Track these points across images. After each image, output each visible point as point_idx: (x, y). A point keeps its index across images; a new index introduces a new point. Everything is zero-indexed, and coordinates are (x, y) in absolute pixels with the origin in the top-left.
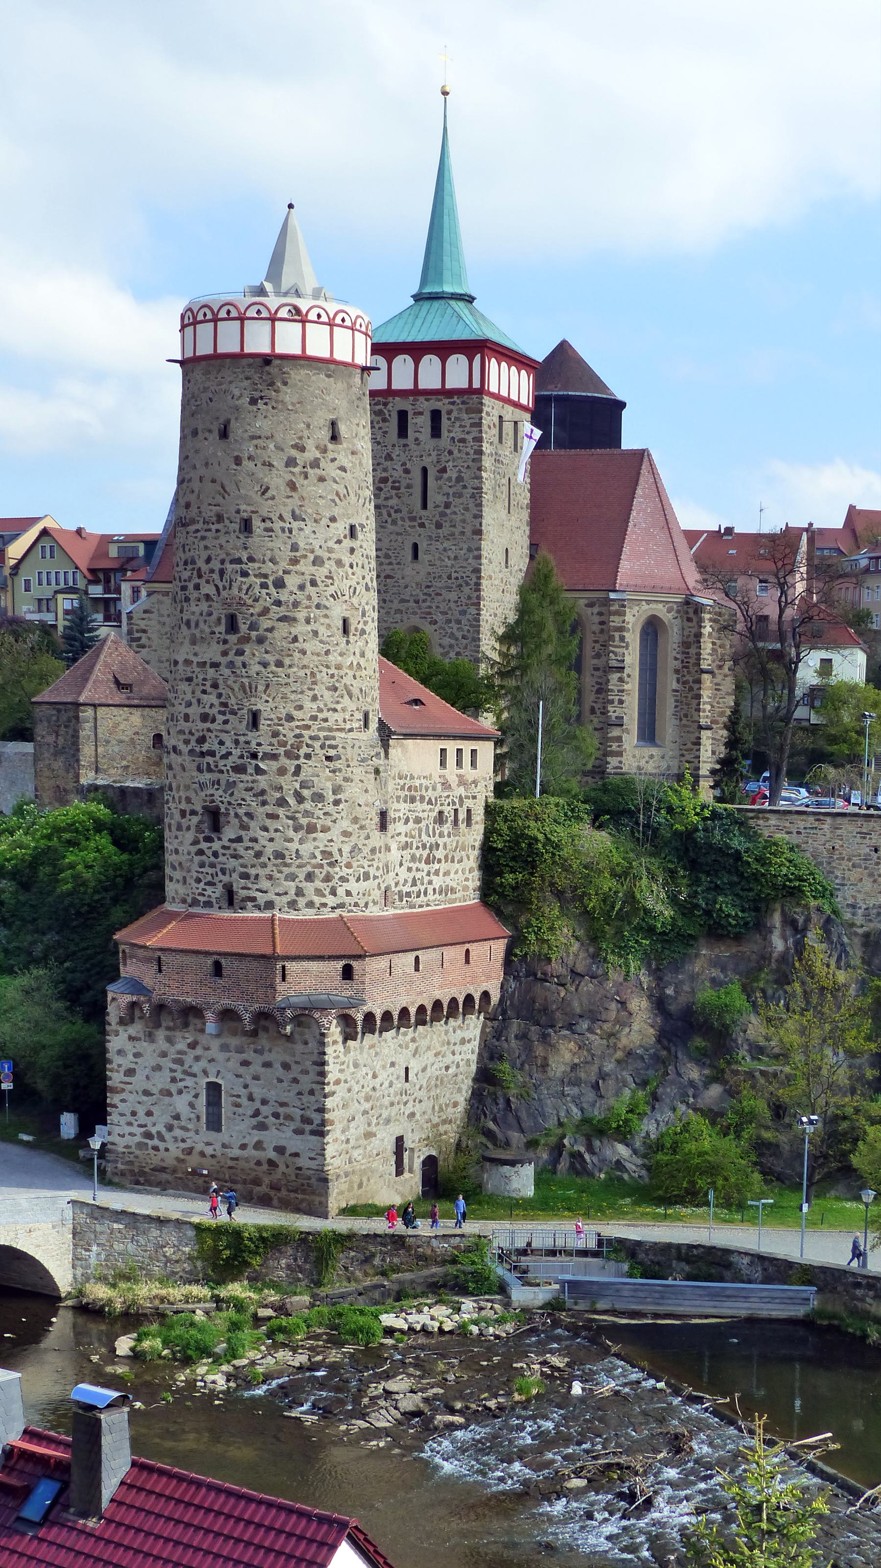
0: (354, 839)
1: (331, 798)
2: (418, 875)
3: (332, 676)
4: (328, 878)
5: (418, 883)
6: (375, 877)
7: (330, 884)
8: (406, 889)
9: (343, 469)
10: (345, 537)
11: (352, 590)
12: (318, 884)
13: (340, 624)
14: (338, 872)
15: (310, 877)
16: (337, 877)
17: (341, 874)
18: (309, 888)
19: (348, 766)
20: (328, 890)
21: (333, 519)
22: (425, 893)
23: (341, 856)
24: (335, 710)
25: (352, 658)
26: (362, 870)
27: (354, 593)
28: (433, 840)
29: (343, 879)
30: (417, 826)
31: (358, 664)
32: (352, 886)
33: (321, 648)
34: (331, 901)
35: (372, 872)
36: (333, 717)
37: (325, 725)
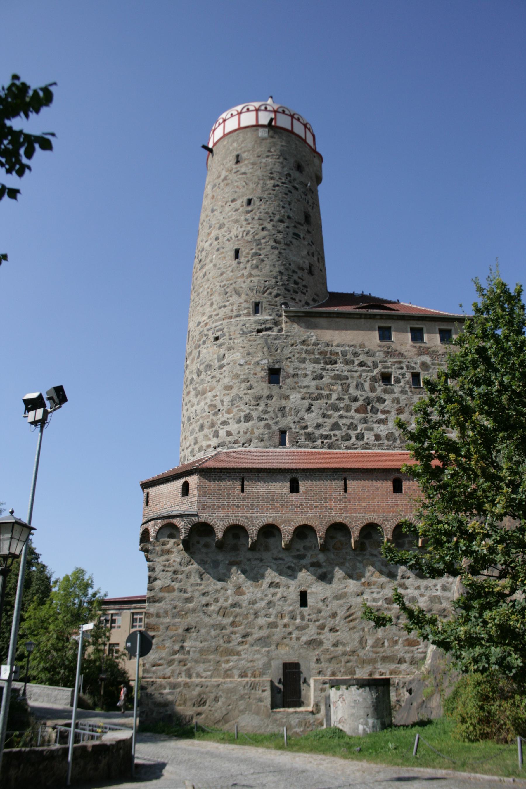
0: (234, 391)
1: (216, 364)
2: (341, 422)
3: (224, 286)
4: (213, 425)
5: (344, 429)
6: (261, 419)
7: (214, 429)
8: (323, 431)
9: (245, 173)
10: (242, 206)
11: (245, 234)
12: (206, 431)
13: (233, 253)
14: (222, 417)
15: (202, 428)
16: (219, 422)
17: (223, 419)
18: (200, 435)
19: (230, 339)
20: (212, 434)
21: (233, 201)
22: (360, 437)
23: (223, 405)
24: (225, 306)
25: (244, 271)
26: (243, 414)
27: (247, 234)
28: (372, 395)
29: (224, 423)
30: (339, 382)
31: (250, 275)
32: (233, 427)
33: (217, 272)
34: (214, 442)
35: (255, 414)
36: (222, 312)
37: (217, 318)
